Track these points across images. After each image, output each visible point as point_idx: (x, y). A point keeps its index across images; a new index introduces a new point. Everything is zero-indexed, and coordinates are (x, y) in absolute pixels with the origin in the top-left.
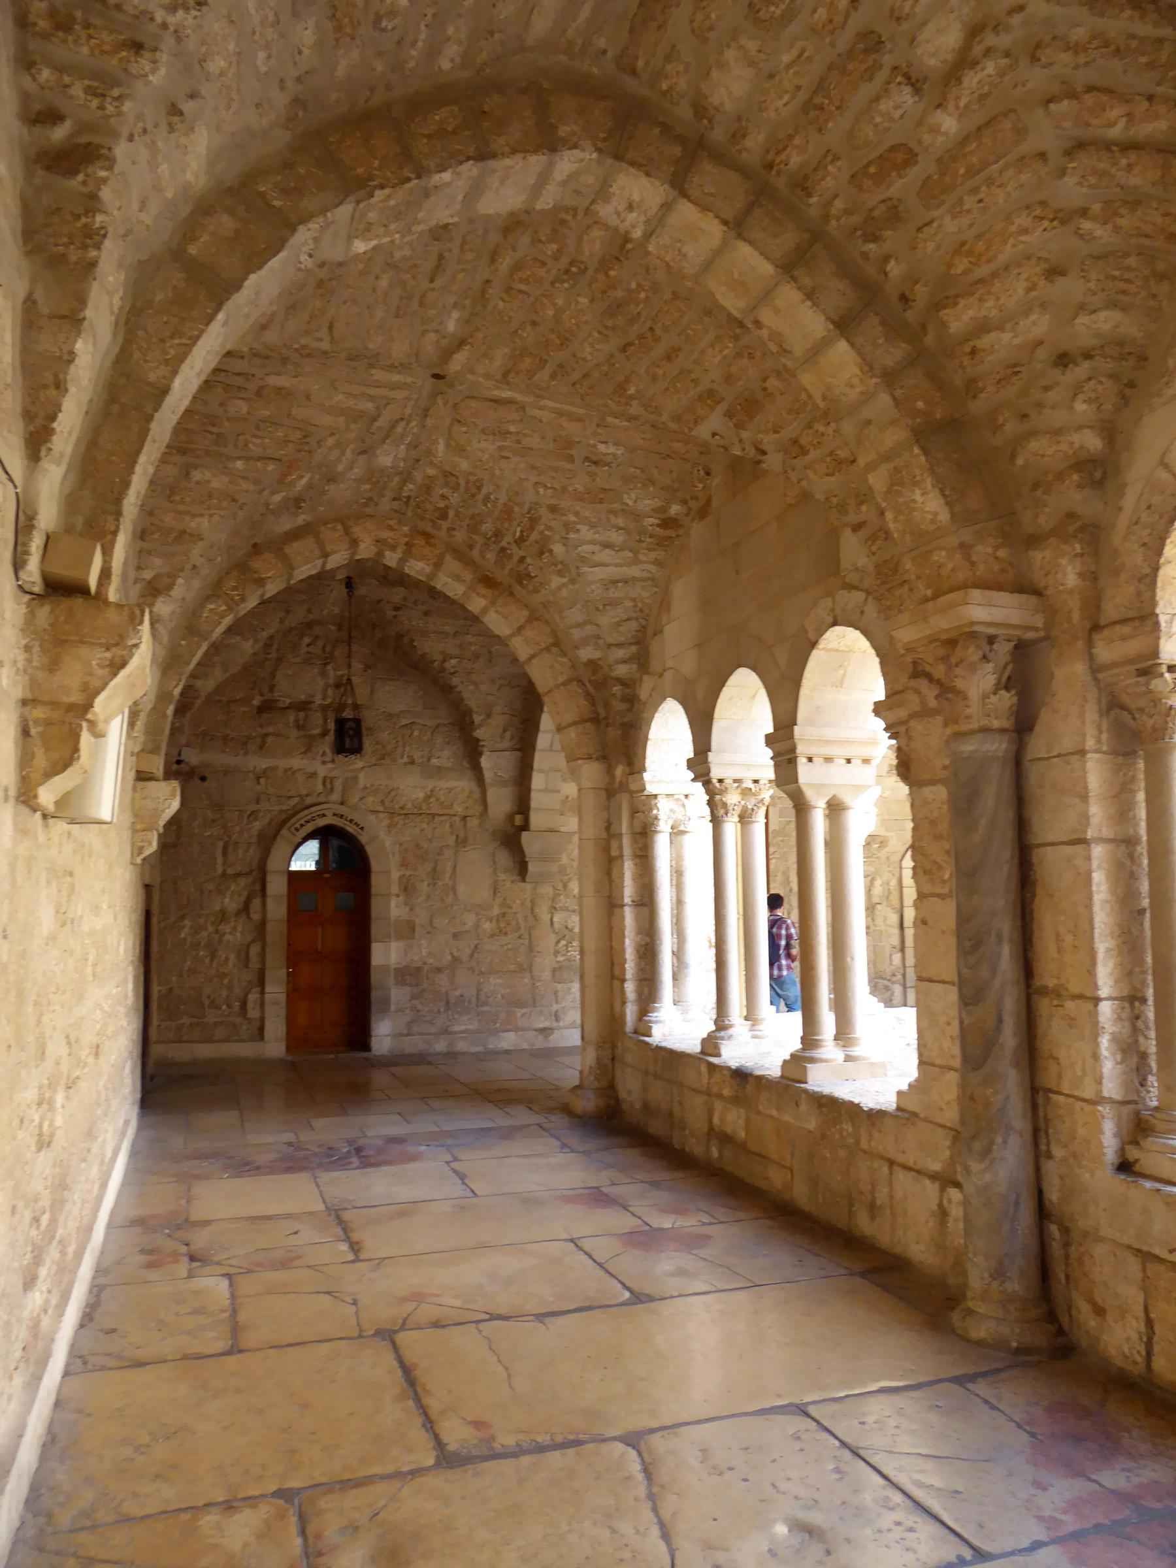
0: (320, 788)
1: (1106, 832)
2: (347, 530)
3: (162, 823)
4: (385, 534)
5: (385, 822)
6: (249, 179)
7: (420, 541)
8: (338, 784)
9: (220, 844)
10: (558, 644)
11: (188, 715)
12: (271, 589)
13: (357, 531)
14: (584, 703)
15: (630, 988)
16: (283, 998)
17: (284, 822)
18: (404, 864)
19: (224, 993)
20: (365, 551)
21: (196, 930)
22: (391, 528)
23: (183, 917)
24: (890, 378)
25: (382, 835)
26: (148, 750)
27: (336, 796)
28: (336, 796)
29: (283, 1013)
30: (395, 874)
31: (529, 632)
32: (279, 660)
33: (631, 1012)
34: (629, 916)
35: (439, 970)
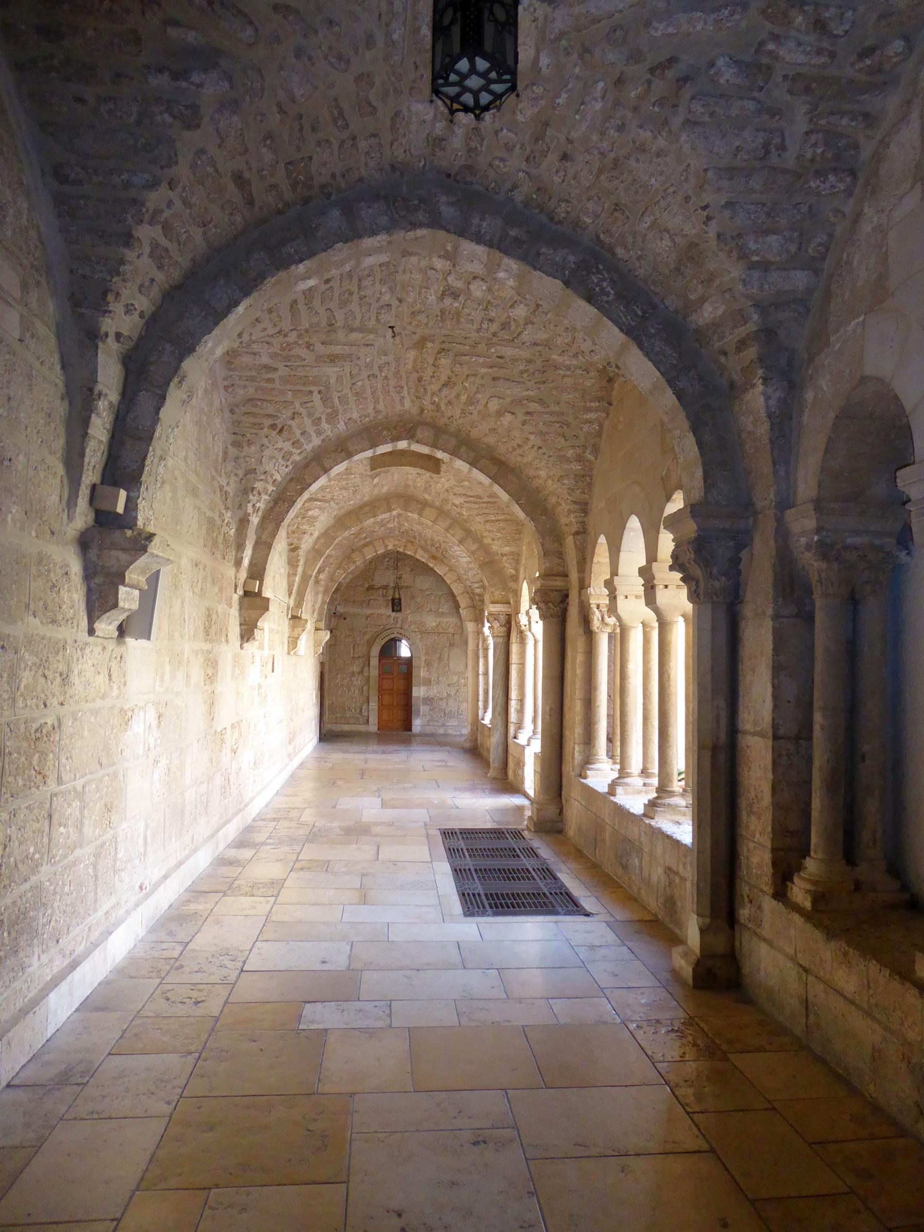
2: (383, 542)
4: (397, 543)
6: (327, 531)
8: (400, 621)
9: (352, 645)
10: (459, 579)
11: (339, 593)
14: (469, 601)
15: (481, 704)
17: (377, 636)
18: (427, 654)
20: (390, 547)
21: (343, 679)
22: (399, 540)
23: (337, 674)
24: (473, 553)
25: (418, 641)
26: (318, 621)
27: (398, 625)
28: (398, 625)
29: (376, 714)
30: (423, 659)
31: (447, 575)
33: (481, 712)
34: (481, 678)
35: (441, 699)
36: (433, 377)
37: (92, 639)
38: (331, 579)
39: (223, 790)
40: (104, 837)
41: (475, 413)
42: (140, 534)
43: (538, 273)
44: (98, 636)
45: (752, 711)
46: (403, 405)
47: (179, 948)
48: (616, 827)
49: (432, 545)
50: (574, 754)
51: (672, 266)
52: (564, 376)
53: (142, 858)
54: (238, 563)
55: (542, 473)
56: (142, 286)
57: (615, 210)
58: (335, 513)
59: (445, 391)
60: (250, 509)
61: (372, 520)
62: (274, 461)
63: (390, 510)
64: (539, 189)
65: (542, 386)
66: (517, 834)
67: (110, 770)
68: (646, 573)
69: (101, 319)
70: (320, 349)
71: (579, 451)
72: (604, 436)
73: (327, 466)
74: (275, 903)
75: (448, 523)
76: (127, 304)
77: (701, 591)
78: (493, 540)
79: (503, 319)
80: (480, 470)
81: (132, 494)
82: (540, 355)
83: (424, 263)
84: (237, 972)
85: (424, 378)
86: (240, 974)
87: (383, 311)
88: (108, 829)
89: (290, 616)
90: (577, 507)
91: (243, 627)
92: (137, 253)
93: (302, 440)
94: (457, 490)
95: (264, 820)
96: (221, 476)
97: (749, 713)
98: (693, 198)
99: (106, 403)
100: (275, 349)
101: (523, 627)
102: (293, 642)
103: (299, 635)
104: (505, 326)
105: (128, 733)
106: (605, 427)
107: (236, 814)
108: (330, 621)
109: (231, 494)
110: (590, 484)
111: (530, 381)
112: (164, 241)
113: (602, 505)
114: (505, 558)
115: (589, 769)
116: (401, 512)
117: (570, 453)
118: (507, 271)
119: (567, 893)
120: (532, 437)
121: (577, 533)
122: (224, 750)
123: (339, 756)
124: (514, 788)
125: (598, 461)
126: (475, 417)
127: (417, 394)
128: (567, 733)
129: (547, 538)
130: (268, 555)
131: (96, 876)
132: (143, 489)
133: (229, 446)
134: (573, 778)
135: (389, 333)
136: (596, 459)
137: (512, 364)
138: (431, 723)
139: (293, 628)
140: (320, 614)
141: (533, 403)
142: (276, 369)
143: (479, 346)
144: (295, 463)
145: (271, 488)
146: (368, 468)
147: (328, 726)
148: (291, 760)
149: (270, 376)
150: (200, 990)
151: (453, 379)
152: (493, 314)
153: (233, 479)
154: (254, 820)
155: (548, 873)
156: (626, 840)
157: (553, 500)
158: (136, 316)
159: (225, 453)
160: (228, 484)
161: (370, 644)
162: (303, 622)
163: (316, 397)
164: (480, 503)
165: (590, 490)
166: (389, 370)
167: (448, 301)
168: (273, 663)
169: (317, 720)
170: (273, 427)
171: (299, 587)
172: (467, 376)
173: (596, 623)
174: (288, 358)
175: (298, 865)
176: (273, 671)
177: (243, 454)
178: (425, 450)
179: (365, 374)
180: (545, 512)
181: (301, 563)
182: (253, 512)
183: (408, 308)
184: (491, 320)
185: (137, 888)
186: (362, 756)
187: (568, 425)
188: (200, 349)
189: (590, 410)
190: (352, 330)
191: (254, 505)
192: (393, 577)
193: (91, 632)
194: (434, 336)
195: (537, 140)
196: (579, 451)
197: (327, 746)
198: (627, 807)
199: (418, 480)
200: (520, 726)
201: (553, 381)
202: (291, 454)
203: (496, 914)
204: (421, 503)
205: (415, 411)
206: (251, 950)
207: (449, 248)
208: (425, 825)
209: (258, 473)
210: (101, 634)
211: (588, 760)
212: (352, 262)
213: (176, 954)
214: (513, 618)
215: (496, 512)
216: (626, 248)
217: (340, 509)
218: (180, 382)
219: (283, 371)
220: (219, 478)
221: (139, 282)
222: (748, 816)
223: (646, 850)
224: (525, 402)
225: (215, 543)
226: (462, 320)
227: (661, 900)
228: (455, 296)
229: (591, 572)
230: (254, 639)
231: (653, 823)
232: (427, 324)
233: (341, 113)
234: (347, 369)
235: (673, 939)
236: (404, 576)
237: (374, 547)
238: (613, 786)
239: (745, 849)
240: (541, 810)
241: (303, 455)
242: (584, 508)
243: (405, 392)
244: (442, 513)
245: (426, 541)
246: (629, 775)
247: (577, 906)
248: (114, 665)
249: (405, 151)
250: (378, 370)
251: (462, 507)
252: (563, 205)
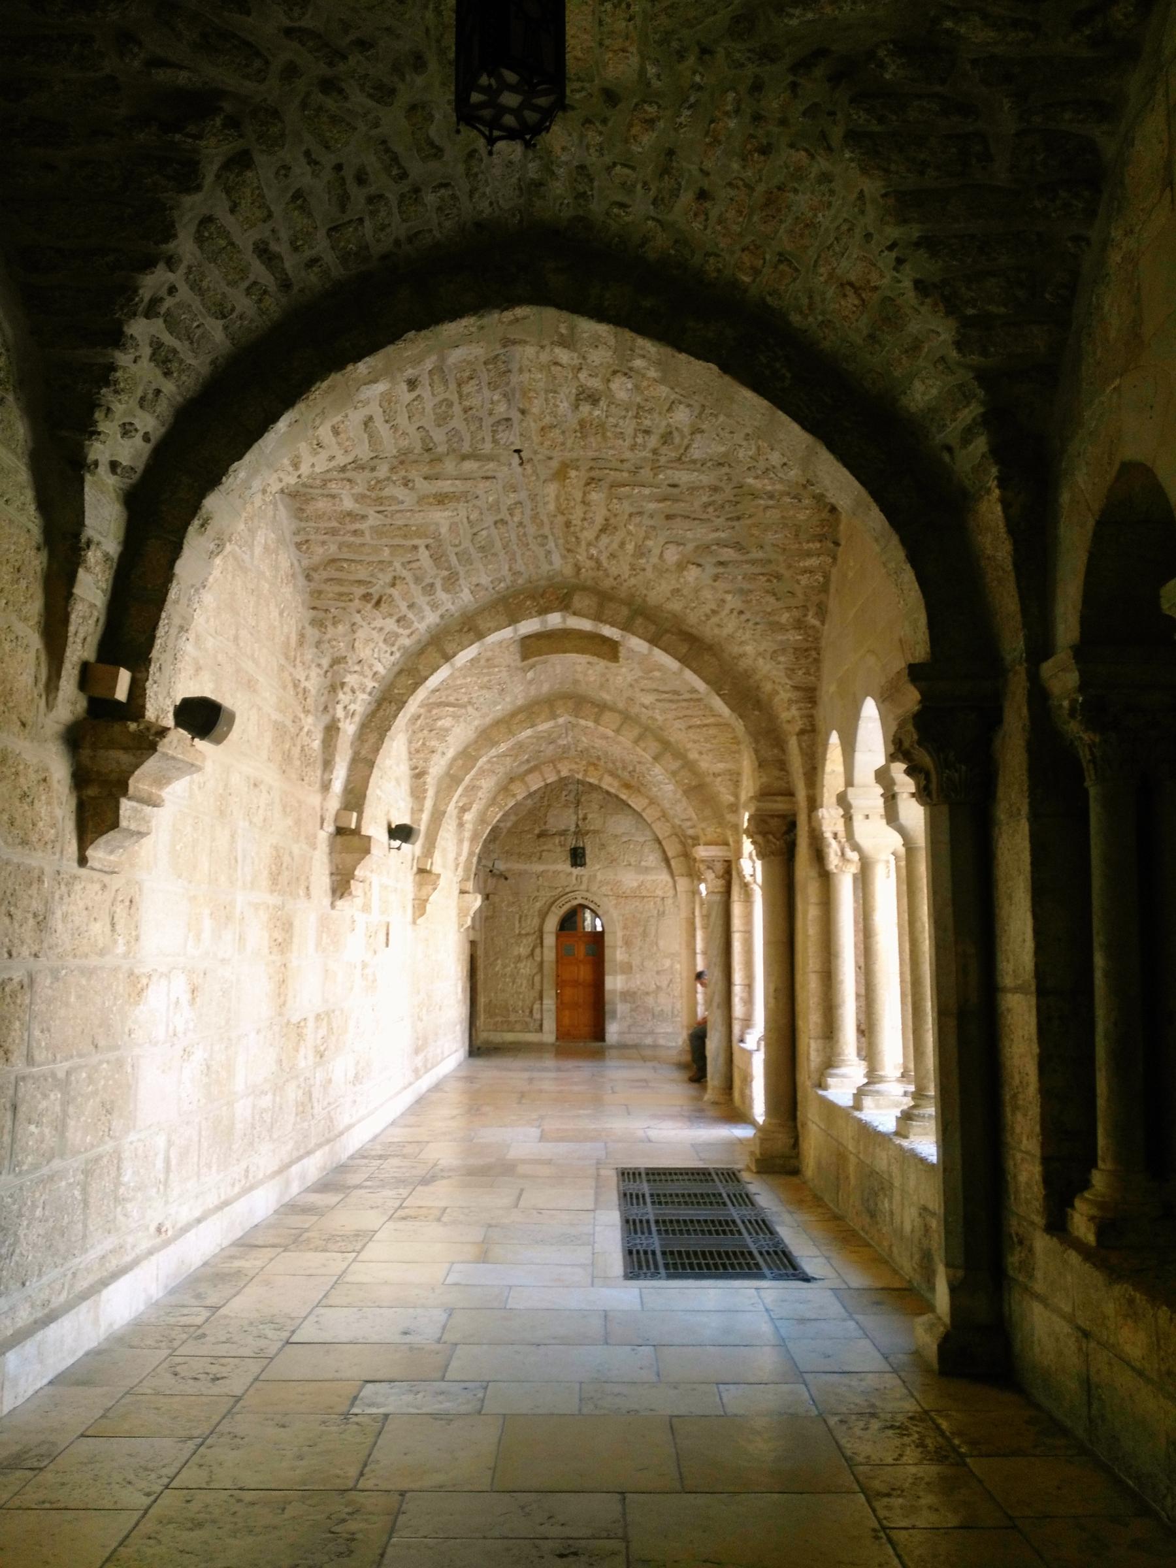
0: (574, 881)
1: (741, 928)
2: (555, 767)
3: (472, 913)
4: (574, 767)
5: (614, 902)
7: (591, 768)
8: (585, 879)
9: (517, 916)
10: (664, 816)
12: (519, 797)
13: (559, 766)
16: (553, 1007)
17: (553, 903)
18: (625, 928)
19: (520, 1004)
20: (564, 773)
21: (504, 966)
22: (577, 763)
23: (497, 959)
24: (674, 774)
26: (465, 879)
27: (583, 887)
28: (583, 887)
29: (554, 1016)
30: (620, 934)
31: (648, 811)
32: (549, 806)
35: (647, 994)
36: (584, 519)
37: (83, 872)
38: (482, 819)
39: (301, 1109)
40: (100, 1149)
41: (649, 569)
42: (148, 729)
43: (683, 357)
44: (92, 869)
45: (1011, 957)
46: (551, 563)
47: (205, 1314)
48: (861, 1156)
49: (624, 768)
50: (809, 1054)
51: (865, 333)
52: (767, 507)
53: (162, 1187)
54: (326, 787)
55: (749, 649)
56: (142, 399)
57: (780, 261)
58: (476, 723)
59: (605, 539)
60: (340, 713)
61: (529, 732)
62: (372, 645)
63: (554, 716)
64: (676, 241)
65: (735, 523)
66: (731, 1176)
67: (112, 1056)
68: (882, 776)
69: (87, 442)
70: (423, 486)
71: (796, 613)
72: (832, 590)
73: (451, 652)
74: (354, 1260)
75: (636, 731)
76: (124, 424)
77: (934, 786)
78: (701, 753)
79: (662, 430)
80: (665, 650)
81: (139, 675)
82: (730, 479)
83: (544, 357)
84: (279, 1344)
85: (574, 522)
86: (283, 1346)
87: (501, 428)
88: (107, 1138)
89: (415, 869)
90: (799, 694)
91: (334, 878)
92: (131, 357)
93: (410, 615)
94: (645, 683)
95: (364, 1157)
96: (294, 666)
97: (1008, 961)
98: (876, 236)
99: (99, 554)
100: (359, 489)
101: (748, 879)
102: (420, 906)
103: (429, 896)
104: (667, 438)
105: (141, 1007)
106: (833, 578)
107: (319, 1146)
108: (485, 882)
109: (313, 692)
110: (817, 661)
111: (718, 517)
112: (168, 339)
113: (833, 688)
114: (719, 779)
115: (831, 1076)
116: (572, 719)
117: (785, 618)
118: (644, 357)
119: (784, 1252)
120: (729, 597)
121: (802, 732)
122: (302, 1051)
123: (490, 1070)
124: (735, 1114)
125: (826, 627)
126: (649, 574)
127: (568, 546)
128: (800, 1023)
129: (762, 742)
130: (369, 776)
131: (86, 1203)
132: (153, 669)
133: (307, 625)
134: (809, 1090)
135: (515, 460)
136: (823, 622)
137: (691, 494)
138: (633, 1030)
139: (420, 885)
140: (467, 869)
141: (726, 549)
142: (364, 517)
143: (642, 471)
144: (404, 649)
145: (370, 684)
146: (518, 657)
147: (483, 1036)
148: (418, 1077)
149: (357, 526)
150: (223, 1365)
151: (612, 521)
152: (647, 422)
153: (314, 672)
154: (352, 1157)
155: (763, 1226)
156: (872, 1173)
157: (768, 687)
158: (138, 440)
159: (302, 636)
160: (307, 678)
161: (543, 916)
162: (433, 877)
163: (423, 554)
164: (678, 701)
165: (818, 669)
166: (522, 513)
167: (585, 408)
168: (388, 934)
169: (466, 1025)
170: (366, 597)
171: (428, 829)
172: (631, 515)
173: (833, 861)
174: (379, 501)
175: (400, 1213)
176: (387, 945)
177: (328, 636)
178: (586, 625)
179: (489, 519)
180: (758, 704)
181: (431, 793)
182: (346, 717)
183: (535, 421)
184: (647, 432)
185: (152, 1229)
186: (526, 1075)
187: (779, 577)
188: (228, 482)
189: (809, 554)
190: (464, 458)
191: (345, 707)
192: (574, 818)
193: (82, 861)
194: (578, 460)
195: (661, 176)
196: (796, 613)
197: (479, 1062)
198: (875, 1124)
199: (590, 672)
200: (748, 1022)
201: (750, 516)
202: (397, 636)
203: (670, 1277)
204: (598, 706)
205: (568, 571)
206: (306, 1318)
207: (564, 331)
208: (598, 1163)
209: (350, 662)
210: (97, 865)
211: (830, 1062)
212: (434, 358)
213: (199, 1320)
214: (734, 866)
215: (700, 713)
216: (801, 312)
217: (483, 716)
218: (202, 526)
219: (374, 520)
220: (292, 669)
221: (139, 394)
222: (1013, 1113)
223: (897, 1184)
224: (714, 547)
225: (287, 758)
226: (609, 434)
227: (917, 1257)
228: (594, 399)
229: (823, 786)
230: (350, 894)
231: (905, 1143)
232: (563, 444)
233: (395, 159)
234: (463, 513)
235: (928, 1307)
236: (590, 816)
237: (542, 774)
238: (860, 1094)
239: (1011, 1163)
240: (766, 1140)
241: (415, 637)
242: (809, 695)
243: (551, 545)
244: (627, 718)
245: (614, 763)
246: (881, 1079)
247: (795, 1268)
248: (120, 911)
249: (491, 204)
250: (507, 513)
251: (653, 709)
252: (712, 260)
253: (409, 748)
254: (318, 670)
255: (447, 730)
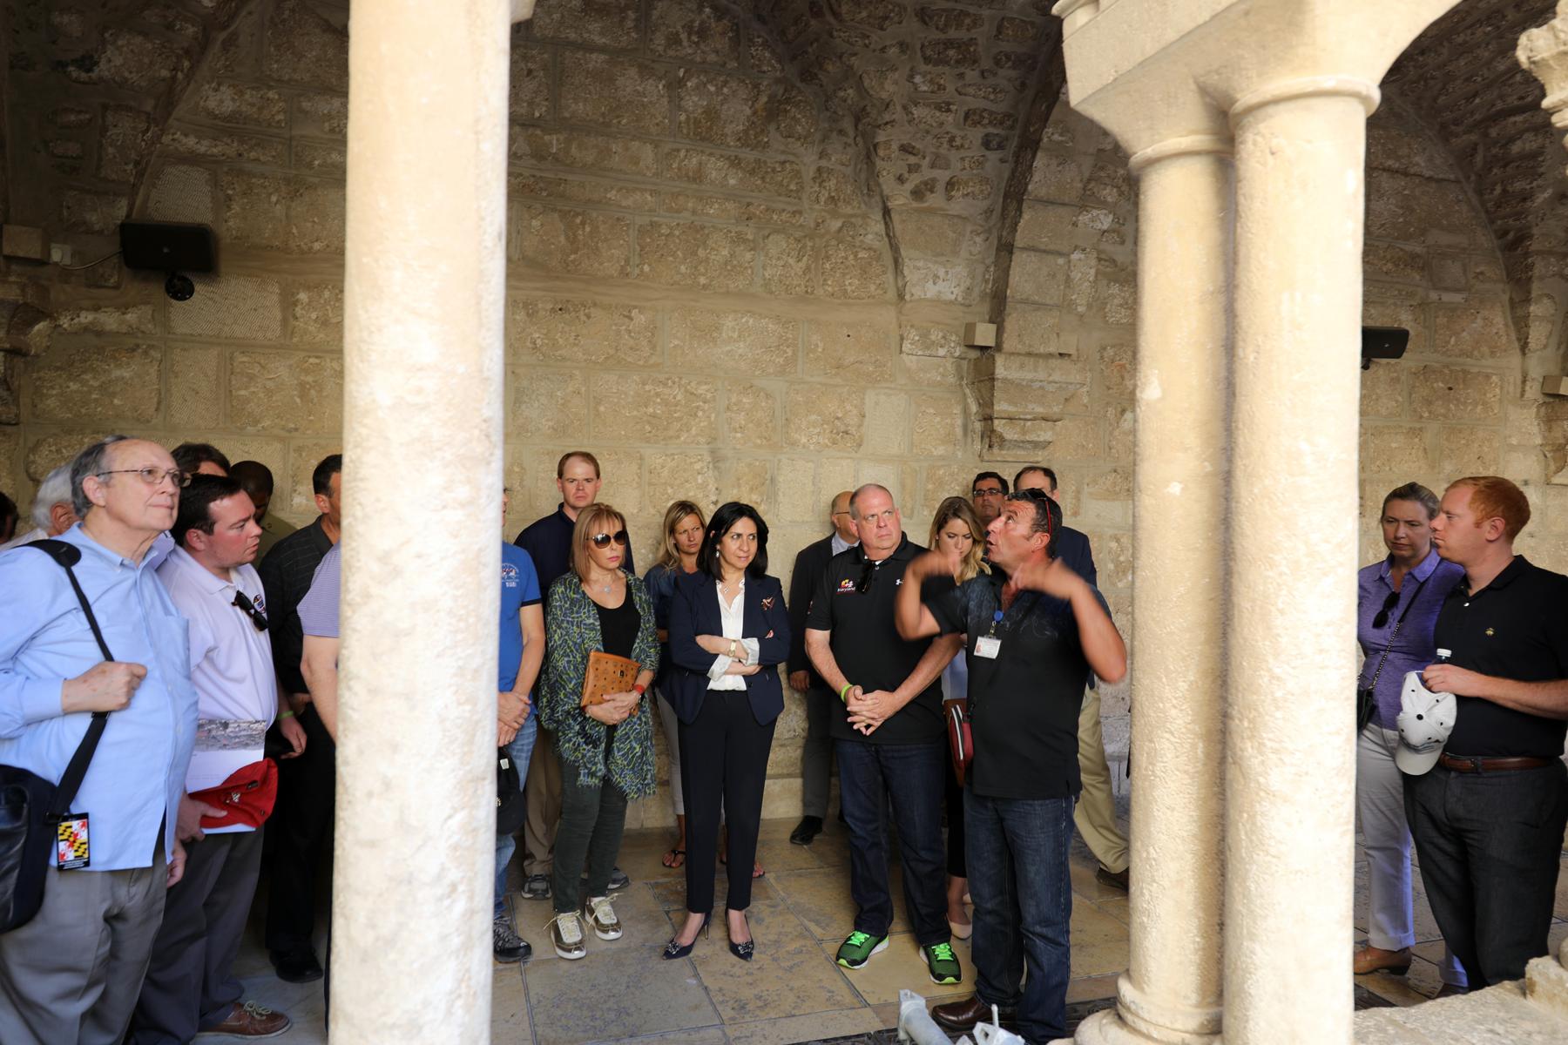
253: (1483, 204)
254: (845, 139)
255: (1534, 155)
